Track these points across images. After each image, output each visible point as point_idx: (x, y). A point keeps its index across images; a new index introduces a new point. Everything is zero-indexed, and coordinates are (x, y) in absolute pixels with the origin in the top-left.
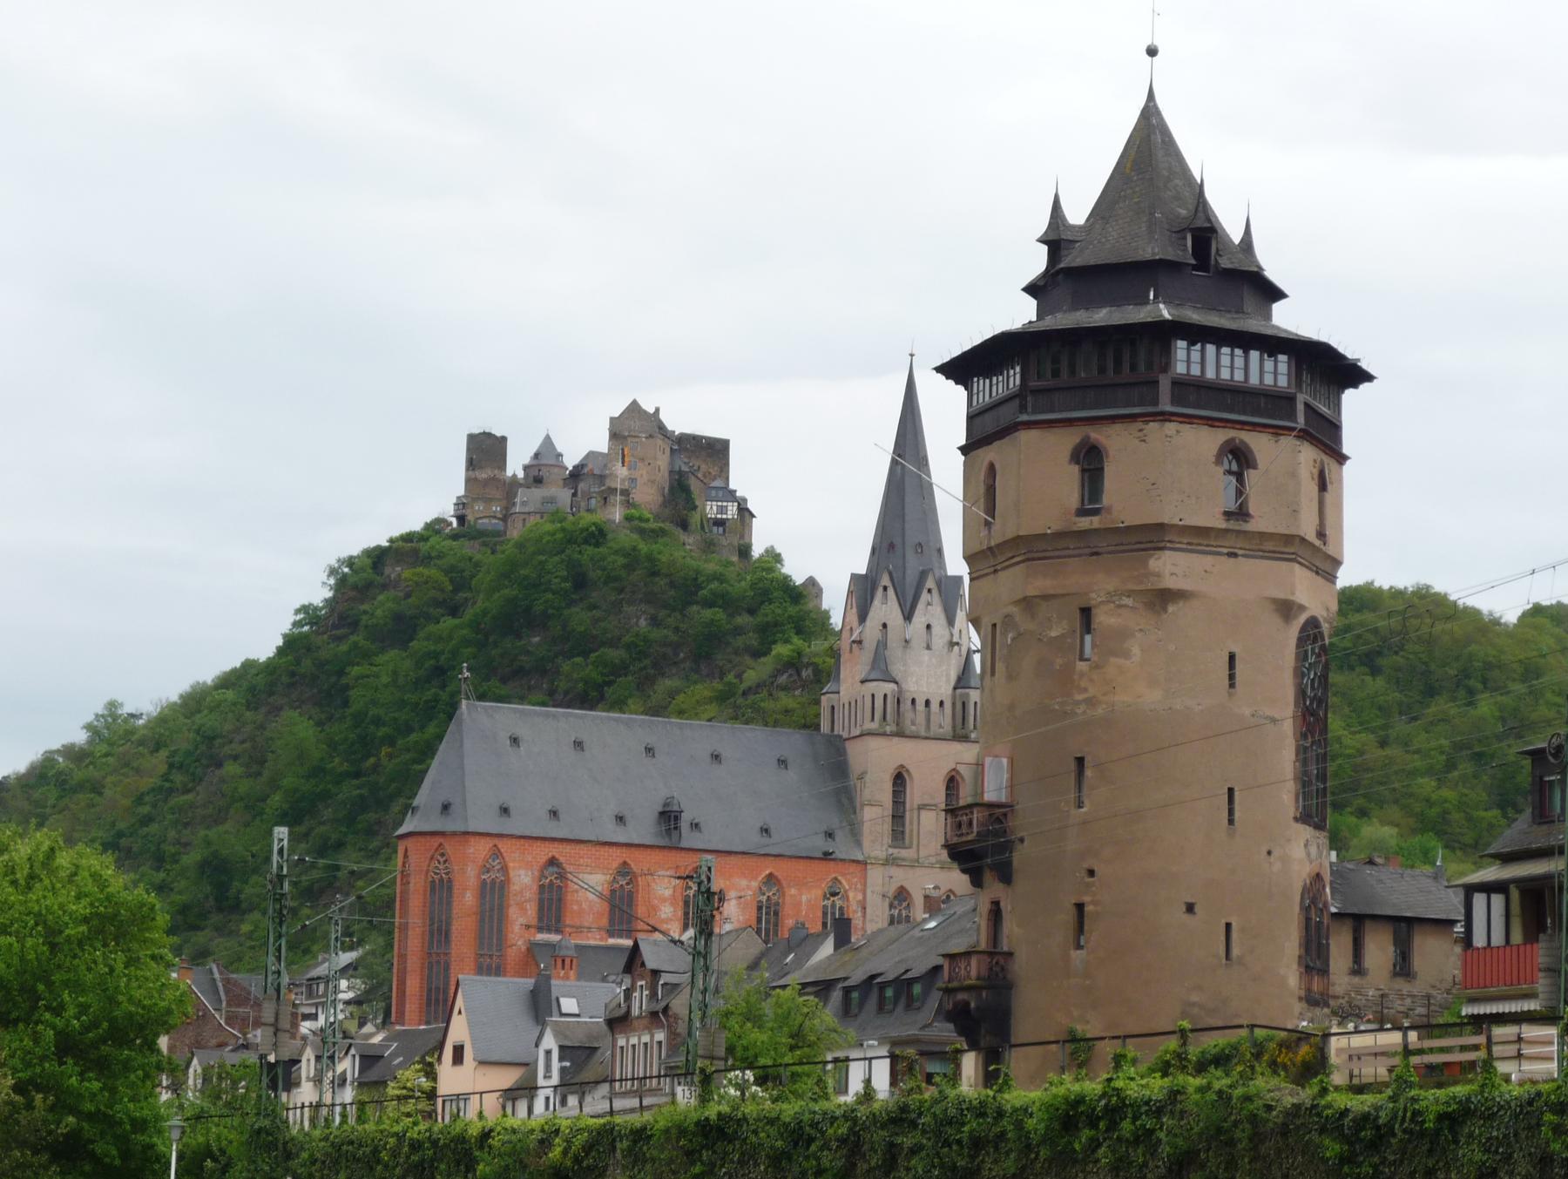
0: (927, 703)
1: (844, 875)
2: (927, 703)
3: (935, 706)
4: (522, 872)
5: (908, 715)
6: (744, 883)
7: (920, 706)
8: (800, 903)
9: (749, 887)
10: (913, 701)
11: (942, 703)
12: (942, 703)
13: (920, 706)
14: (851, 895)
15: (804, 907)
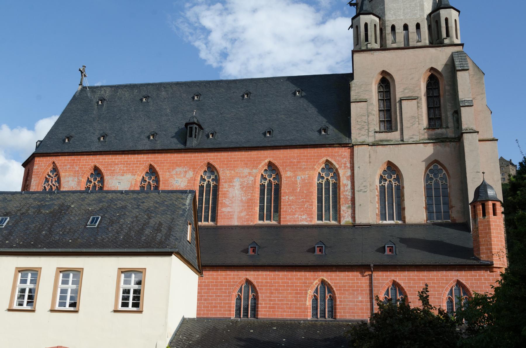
0: (406, 27)
1: (332, 156)
2: (406, 27)
3: (412, 28)
4: (71, 179)
5: (389, 38)
6: (246, 171)
7: (399, 29)
8: (295, 183)
9: (250, 174)
10: (393, 28)
11: (418, 26)
12: (418, 26)
13: (399, 29)
14: (341, 172)
15: (299, 185)
